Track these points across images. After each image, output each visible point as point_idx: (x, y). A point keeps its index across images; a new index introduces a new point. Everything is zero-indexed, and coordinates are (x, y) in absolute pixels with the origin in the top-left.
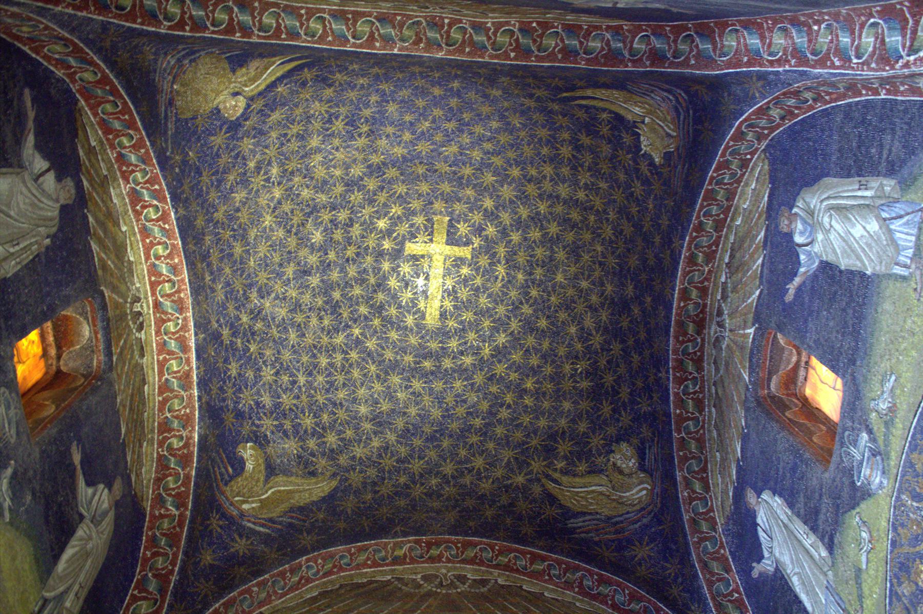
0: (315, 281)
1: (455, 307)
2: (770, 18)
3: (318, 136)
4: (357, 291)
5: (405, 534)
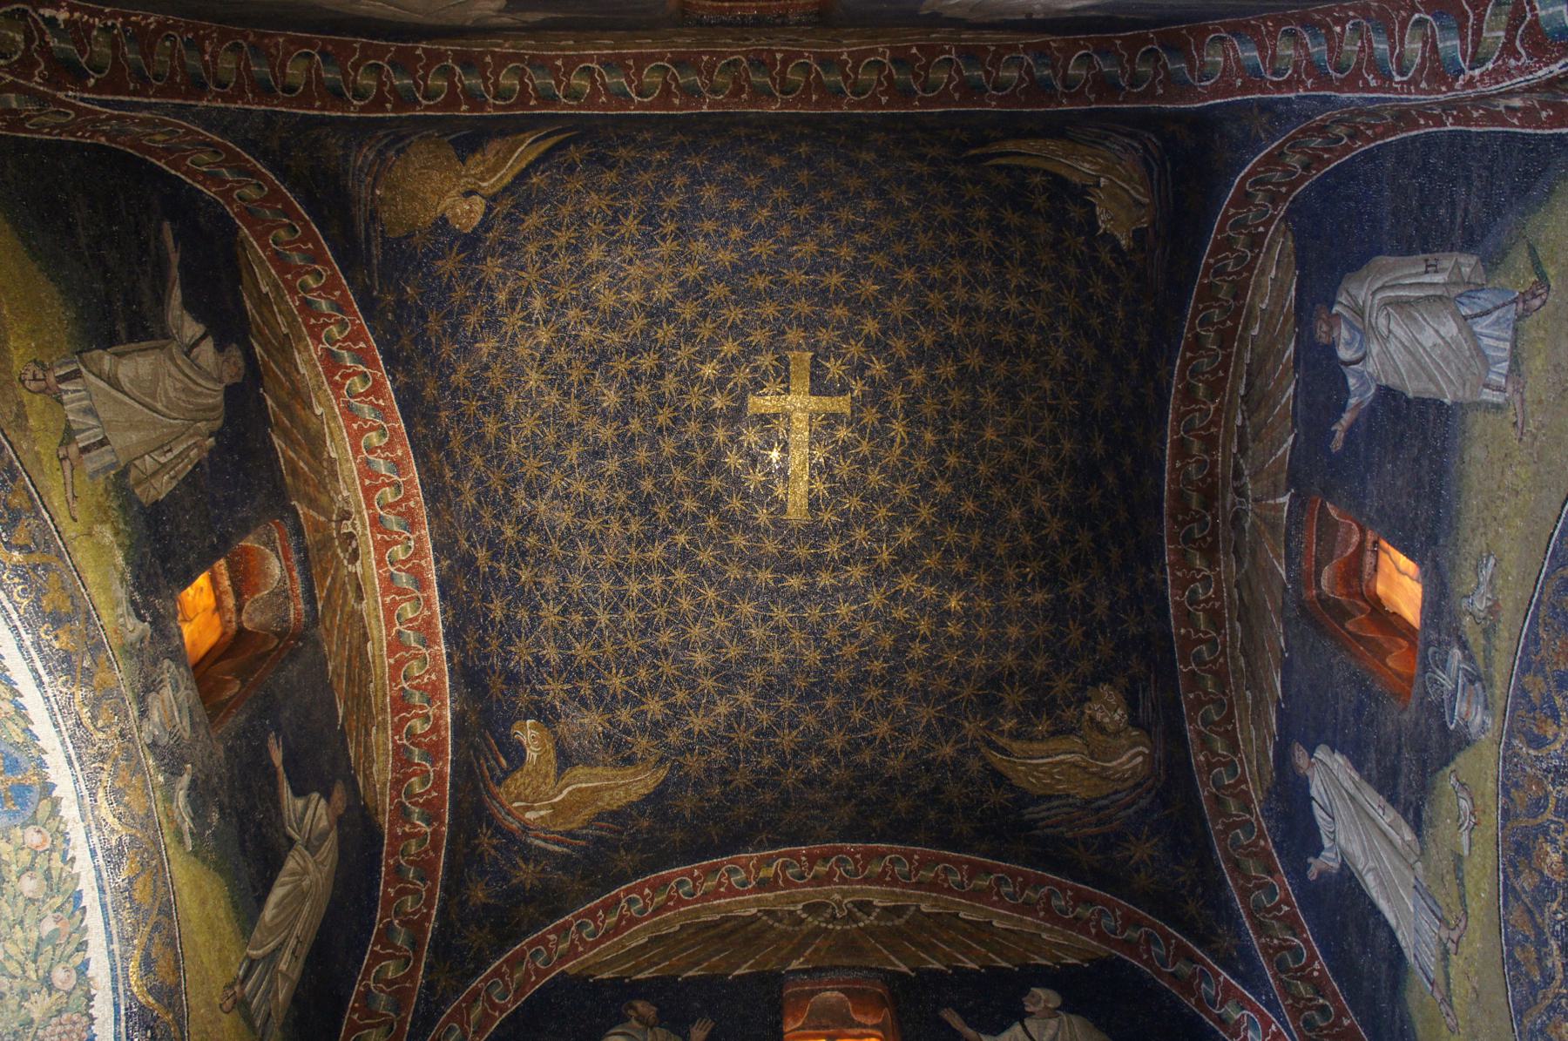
0: (612, 466)
1: (831, 490)
2: (1269, 18)
3: (600, 244)
4: (679, 476)
5: (775, 844)
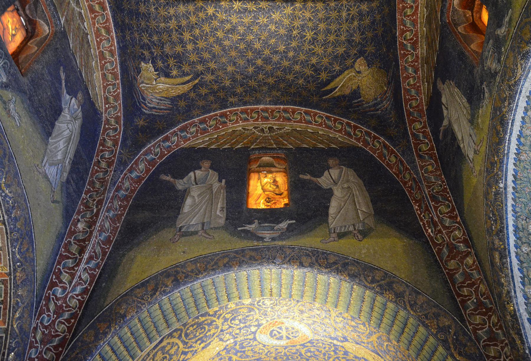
3: (320, 30)
